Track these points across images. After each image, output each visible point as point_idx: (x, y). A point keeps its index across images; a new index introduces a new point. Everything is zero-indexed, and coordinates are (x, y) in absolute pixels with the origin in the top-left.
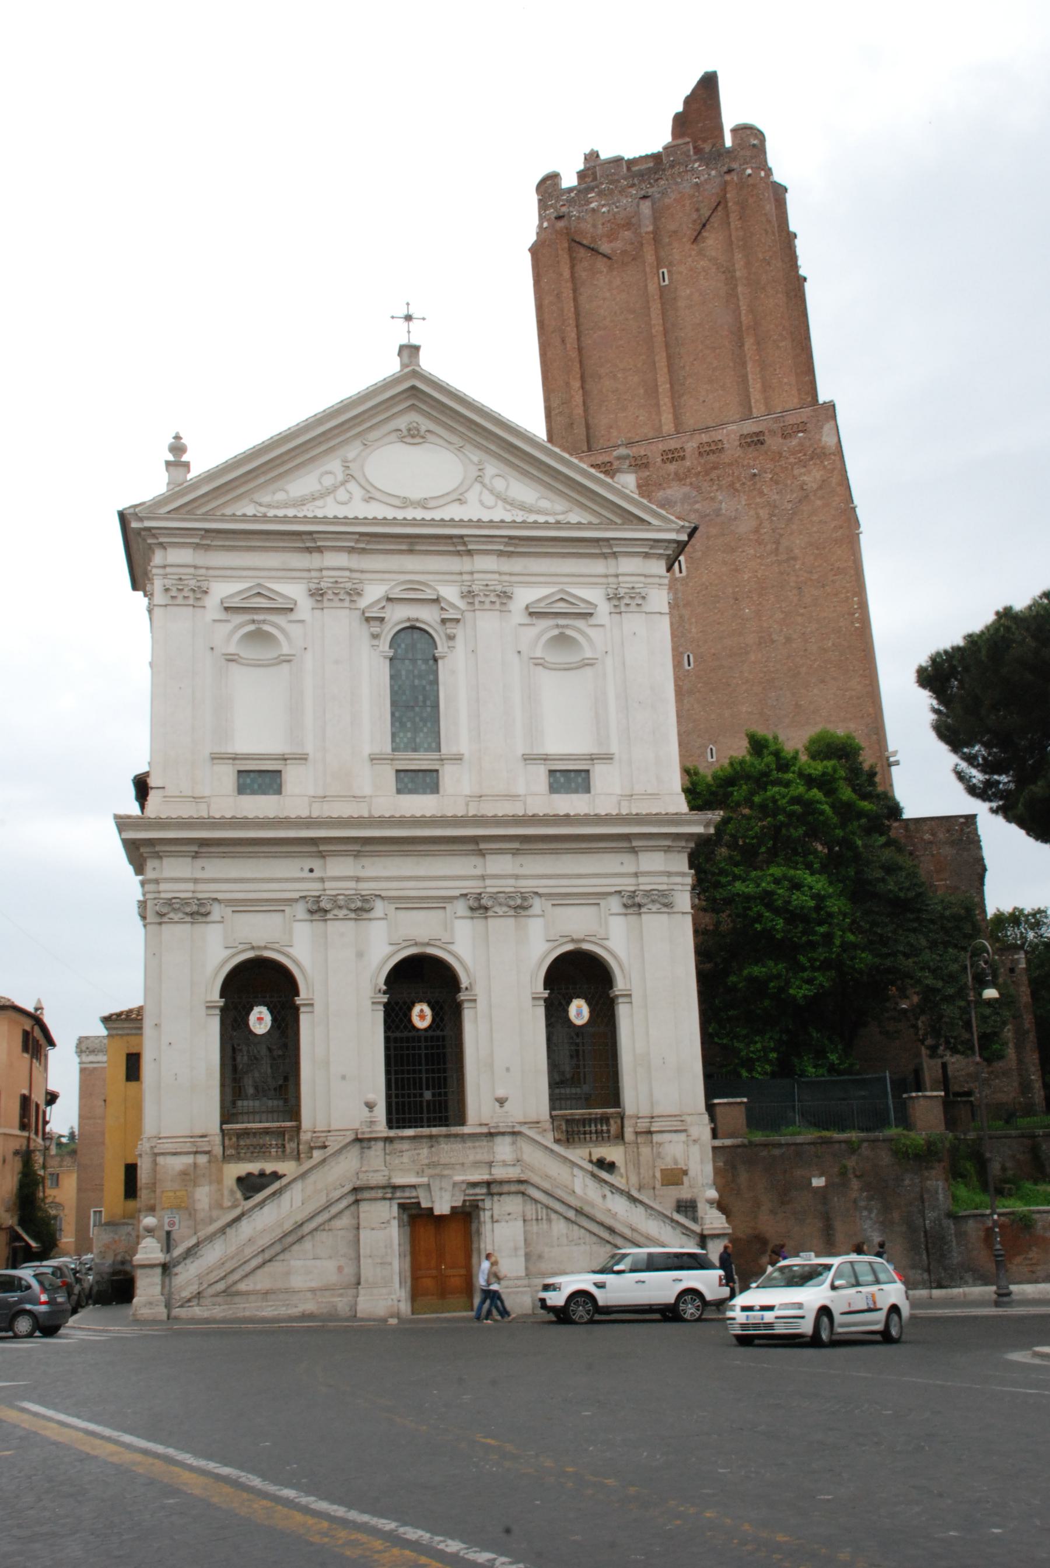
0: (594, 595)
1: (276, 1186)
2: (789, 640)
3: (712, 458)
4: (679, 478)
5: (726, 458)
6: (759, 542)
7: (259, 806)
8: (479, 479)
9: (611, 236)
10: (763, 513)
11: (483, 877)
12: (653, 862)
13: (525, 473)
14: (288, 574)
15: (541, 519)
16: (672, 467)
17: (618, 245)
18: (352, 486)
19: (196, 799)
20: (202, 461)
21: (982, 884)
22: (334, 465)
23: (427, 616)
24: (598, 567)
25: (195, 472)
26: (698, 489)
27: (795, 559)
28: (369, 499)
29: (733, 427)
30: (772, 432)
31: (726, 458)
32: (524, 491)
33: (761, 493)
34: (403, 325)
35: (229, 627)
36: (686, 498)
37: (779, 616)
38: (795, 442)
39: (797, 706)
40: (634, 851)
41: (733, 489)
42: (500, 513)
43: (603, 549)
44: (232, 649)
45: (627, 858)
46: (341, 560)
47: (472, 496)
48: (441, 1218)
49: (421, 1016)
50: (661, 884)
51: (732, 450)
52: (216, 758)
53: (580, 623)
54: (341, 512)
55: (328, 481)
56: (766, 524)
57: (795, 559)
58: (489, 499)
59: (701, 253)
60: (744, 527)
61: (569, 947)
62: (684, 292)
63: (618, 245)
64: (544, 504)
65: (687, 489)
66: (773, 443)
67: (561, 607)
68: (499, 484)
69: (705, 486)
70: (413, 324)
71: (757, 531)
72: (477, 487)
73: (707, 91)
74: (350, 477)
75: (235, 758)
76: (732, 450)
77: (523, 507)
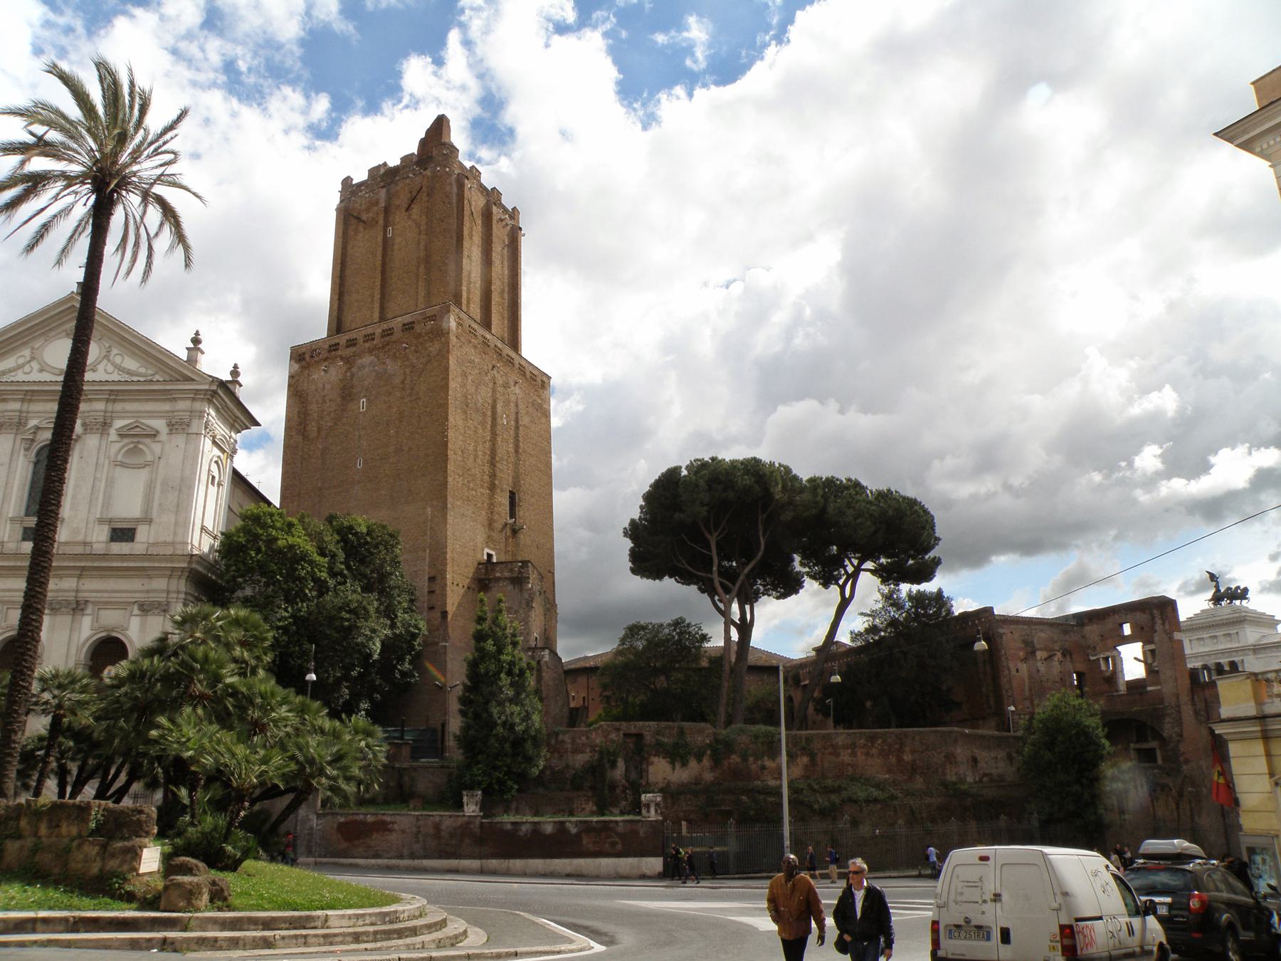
0: (160, 424)
2: (410, 449)
3: (387, 338)
4: (370, 351)
5: (394, 338)
7: (118, 548)
8: (107, 357)
9: (368, 210)
10: (408, 371)
11: (148, 591)
12: (160, 584)
13: (134, 353)
14: (152, 415)
15: (135, 379)
16: (367, 345)
18: (35, 365)
19: (85, 544)
22: (27, 352)
24: (166, 407)
26: (378, 357)
28: (41, 371)
29: (399, 319)
30: (419, 322)
31: (394, 338)
32: (131, 364)
33: (408, 359)
35: (119, 445)
40: (149, 577)
41: (395, 357)
42: (115, 377)
43: (167, 396)
44: (119, 458)
45: (145, 581)
46: (17, 406)
47: (101, 367)
50: (161, 597)
51: (398, 334)
52: (101, 521)
54: (27, 378)
55: (21, 361)
58: (110, 368)
59: (409, 217)
61: (104, 634)
62: (398, 240)
64: (143, 370)
66: (418, 328)
67: (137, 431)
68: (118, 360)
69: (381, 355)
71: (403, 382)
72: (105, 361)
74: (33, 358)
75: (110, 521)
76: (398, 334)
77: (129, 373)
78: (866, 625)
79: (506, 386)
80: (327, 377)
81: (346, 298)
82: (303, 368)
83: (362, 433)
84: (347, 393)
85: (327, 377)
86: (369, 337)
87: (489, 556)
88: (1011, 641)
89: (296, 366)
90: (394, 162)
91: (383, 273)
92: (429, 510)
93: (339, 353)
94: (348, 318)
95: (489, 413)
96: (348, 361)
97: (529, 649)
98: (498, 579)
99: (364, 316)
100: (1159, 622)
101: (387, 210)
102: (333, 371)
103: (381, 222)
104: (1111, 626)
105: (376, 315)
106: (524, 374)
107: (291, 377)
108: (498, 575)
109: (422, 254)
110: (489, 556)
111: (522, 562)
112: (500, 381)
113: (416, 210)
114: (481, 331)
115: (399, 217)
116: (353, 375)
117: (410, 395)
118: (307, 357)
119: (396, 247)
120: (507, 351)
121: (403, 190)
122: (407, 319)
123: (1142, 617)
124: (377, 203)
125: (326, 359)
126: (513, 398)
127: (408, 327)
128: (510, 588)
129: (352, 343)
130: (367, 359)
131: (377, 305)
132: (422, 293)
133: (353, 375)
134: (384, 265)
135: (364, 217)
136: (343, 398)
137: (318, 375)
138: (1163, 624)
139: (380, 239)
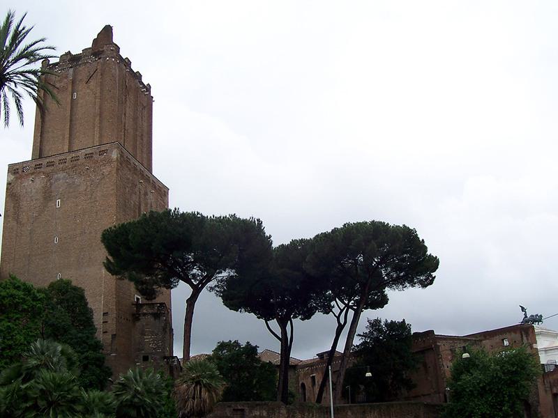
2: (91, 233)
3: (75, 162)
4: (63, 170)
5: (79, 162)
16: (61, 166)
17: (62, 84)
27: (97, 201)
33: (89, 176)
36: (64, 177)
37: (89, 223)
39: (90, 258)
51: (82, 160)
56: (89, 188)
57: (97, 201)
60: (82, 188)
62: (81, 101)
65: (65, 174)
66: (96, 157)
73: (108, 31)
76: (82, 160)
78: (361, 341)
79: (146, 194)
80: (34, 185)
81: (46, 135)
82: (17, 178)
83: (58, 221)
84: (48, 196)
85: (34, 185)
86: (63, 161)
87: (138, 299)
88: (444, 347)
89: (12, 177)
90: (76, 51)
91: (71, 121)
93: (42, 169)
94: (48, 149)
95: (137, 211)
96: (48, 175)
97: (165, 358)
98: (145, 314)
99: (57, 146)
100: (525, 338)
101: (73, 82)
102: (38, 181)
103: (70, 89)
104: (498, 340)
105: (66, 149)
106: (155, 187)
107: (9, 184)
108: (145, 311)
109: (97, 111)
110: (138, 299)
111: (160, 304)
112: (142, 192)
113: (92, 83)
114: (133, 160)
115: (80, 86)
116: (51, 184)
117: (91, 198)
118: (20, 171)
119: (79, 105)
121: (83, 71)
122: (89, 151)
123: (517, 336)
124: (66, 77)
125: (32, 174)
126: (149, 201)
127: (89, 156)
128: (152, 319)
129: (50, 164)
130: (61, 175)
131: (67, 141)
132: (97, 135)
133: (51, 184)
134: (71, 115)
135: (58, 85)
137: (27, 183)
138: (527, 339)
139: (69, 99)
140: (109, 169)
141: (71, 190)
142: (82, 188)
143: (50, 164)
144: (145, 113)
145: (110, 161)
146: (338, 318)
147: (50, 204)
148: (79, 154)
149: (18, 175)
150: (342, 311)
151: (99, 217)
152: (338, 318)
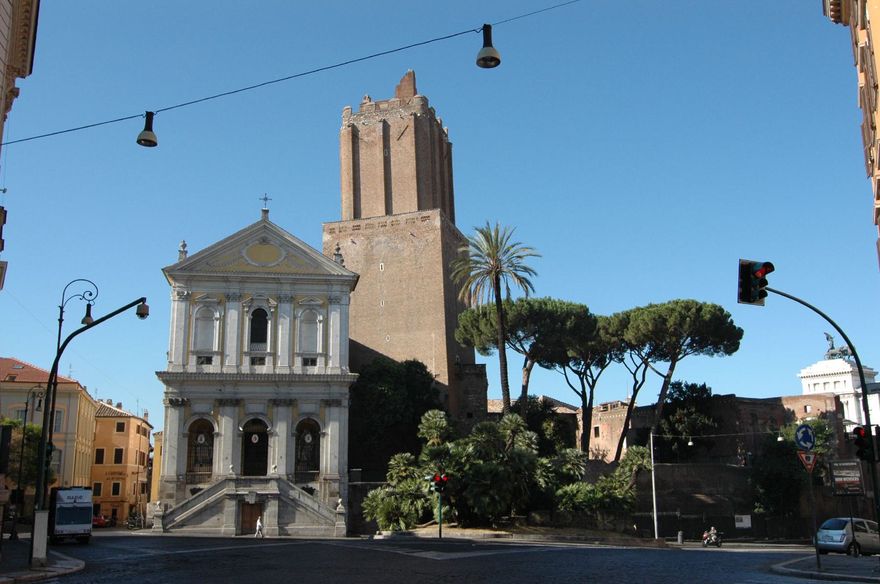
1: (199, 493)
2: (418, 298)
6: (410, 260)
16: (382, 229)
20: (192, 251)
21: (486, 390)
23: (265, 306)
25: (188, 255)
34: (263, 202)
36: (386, 241)
38: (425, 223)
48: (252, 505)
49: (255, 439)
51: (403, 223)
53: (317, 308)
60: (406, 254)
63: (371, 139)
70: (268, 202)
92: (433, 335)
98: (467, 374)
116: (372, 247)
118: (337, 231)
120: (451, 224)
122: (409, 216)
125: (351, 235)
130: (382, 238)
136: (367, 261)
140: (432, 236)
141: (395, 255)
142: (406, 254)
143: (371, 226)
144: (446, 162)
145: (434, 229)
146: (635, 375)
147: (373, 267)
148: (399, 218)
149: (334, 235)
150: (638, 368)
151: (425, 283)
152: (635, 375)
